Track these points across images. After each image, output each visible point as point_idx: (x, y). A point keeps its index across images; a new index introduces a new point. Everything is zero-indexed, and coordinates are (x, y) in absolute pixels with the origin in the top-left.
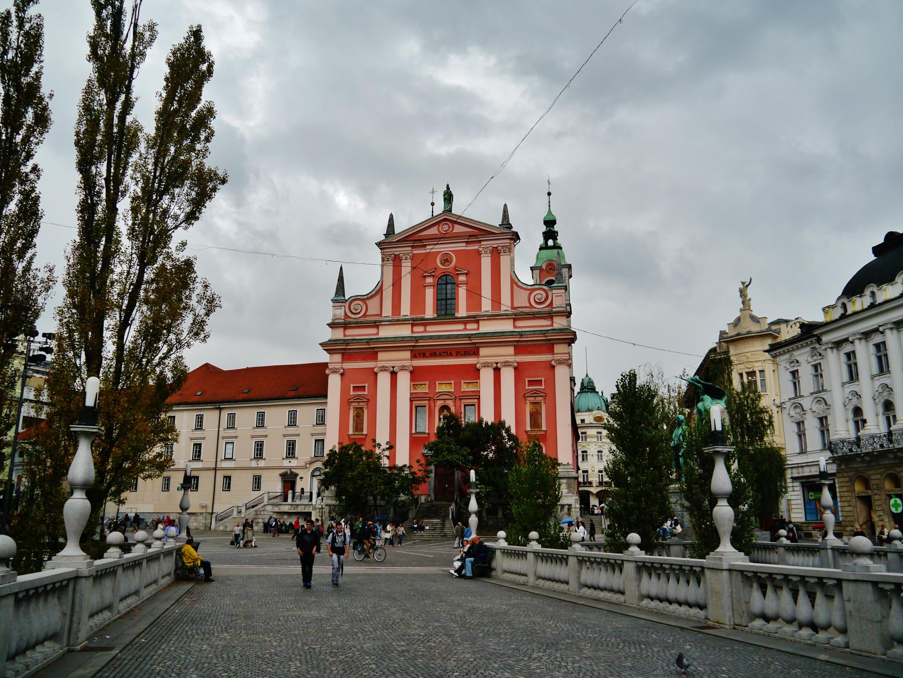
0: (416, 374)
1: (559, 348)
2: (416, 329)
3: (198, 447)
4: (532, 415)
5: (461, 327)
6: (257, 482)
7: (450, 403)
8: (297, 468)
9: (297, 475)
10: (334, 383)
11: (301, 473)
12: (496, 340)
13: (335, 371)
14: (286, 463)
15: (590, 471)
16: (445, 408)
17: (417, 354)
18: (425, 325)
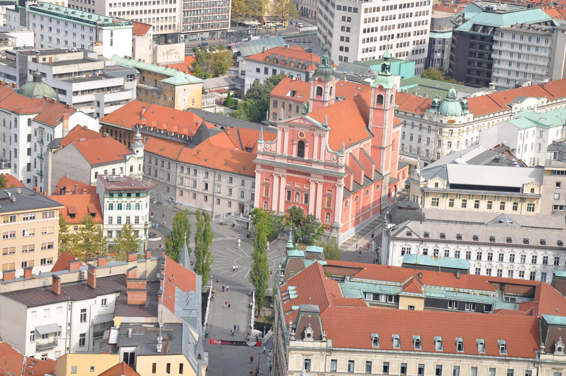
0: (288, 179)
1: (338, 180)
2: (289, 161)
3: (207, 185)
4: (328, 202)
5: (306, 164)
6: (230, 204)
7: (299, 192)
8: (245, 202)
9: (244, 205)
10: (258, 176)
11: (246, 205)
12: (317, 172)
13: (257, 171)
14: (240, 200)
15: (441, 154)
16: (297, 193)
17: (288, 171)
18: (292, 160)
